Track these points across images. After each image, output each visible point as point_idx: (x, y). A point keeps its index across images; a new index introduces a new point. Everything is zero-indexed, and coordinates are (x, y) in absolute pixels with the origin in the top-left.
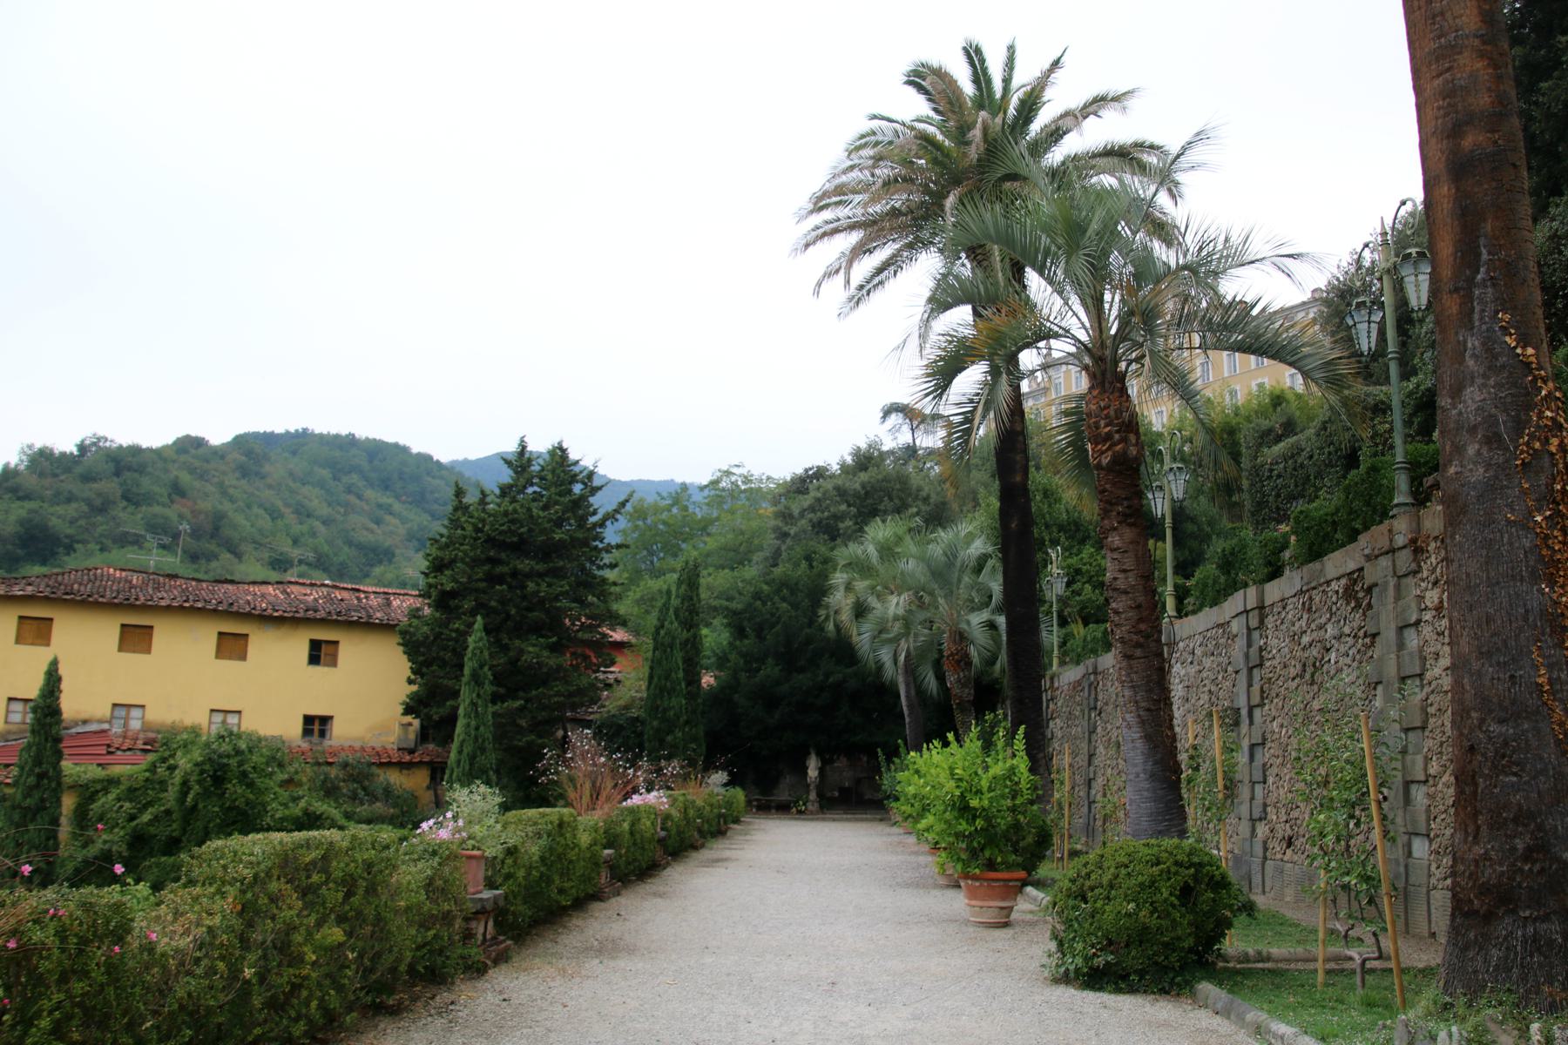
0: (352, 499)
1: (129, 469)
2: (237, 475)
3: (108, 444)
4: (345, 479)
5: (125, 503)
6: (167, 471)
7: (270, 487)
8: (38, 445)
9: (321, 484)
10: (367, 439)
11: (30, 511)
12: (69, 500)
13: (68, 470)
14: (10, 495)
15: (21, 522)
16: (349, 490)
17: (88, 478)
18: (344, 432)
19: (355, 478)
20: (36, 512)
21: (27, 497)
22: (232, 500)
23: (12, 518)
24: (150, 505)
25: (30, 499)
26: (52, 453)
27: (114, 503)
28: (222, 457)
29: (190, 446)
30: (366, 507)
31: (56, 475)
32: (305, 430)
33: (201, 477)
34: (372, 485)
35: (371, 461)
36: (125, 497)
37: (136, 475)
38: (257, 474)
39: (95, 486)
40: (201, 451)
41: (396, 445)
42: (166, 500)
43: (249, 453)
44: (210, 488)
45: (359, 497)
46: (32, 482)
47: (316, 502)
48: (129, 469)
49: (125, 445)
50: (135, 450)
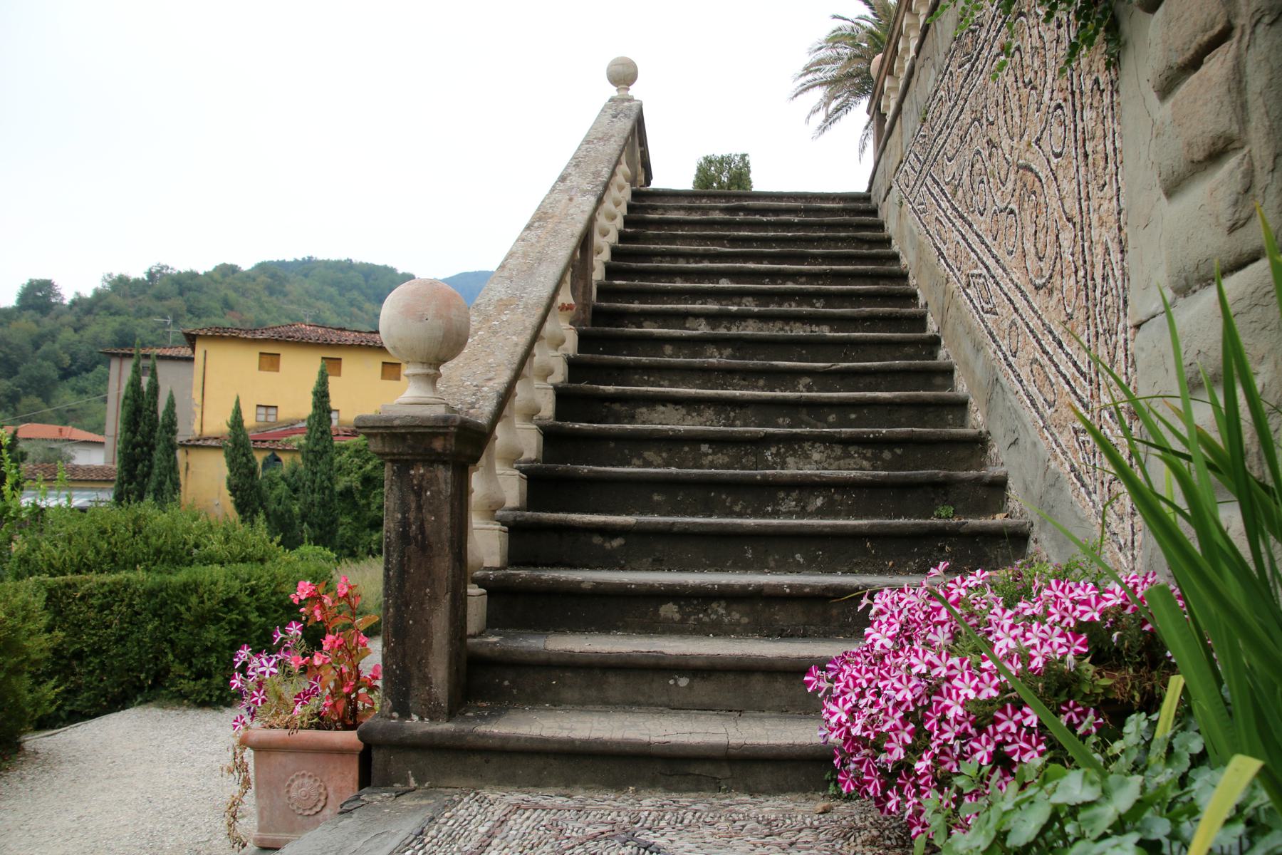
0: (355, 310)
1: (190, 289)
2: (267, 293)
3: (169, 271)
4: (348, 295)
5: (191, 316)
6: (217, 290)
7: (292, 302)
8: (116, 274)
9: (331, 299)
10: (361, 263)
11: (122, 324)
12: (149, 315)
13: (144, 292)
14: (105, 312)
15: (116, 332)
16: (352, 304)
17: (160, 297)
18: (343, 258)
19: (355, 294)
20: (125, 324)
21: (117, 313)
22: (268, 312)
23: (109, 329)
24: (208, 316)
25: (120, 315)
26: (128, 280)
27: (182, 316)
28: (254, 280)
29: (227, 271)
30: (365, 317)
31: (134, 296)
32: (310, 258)
33: (243, 295)
34: (369, 300)
35: (366, 281)
36: (190, 311)
37: (196, 294)
38: (281, 292)
39: (166, 303)
40: (236, 275)
41: (385, 268)
42: (220, 313)
43: (274, 276)
44: (251, 303)
45: (360, 309)
46: (118, 301)
47: (328, 313)
48: (190, 289)
49: (183, 271)
50: (193, 275)
